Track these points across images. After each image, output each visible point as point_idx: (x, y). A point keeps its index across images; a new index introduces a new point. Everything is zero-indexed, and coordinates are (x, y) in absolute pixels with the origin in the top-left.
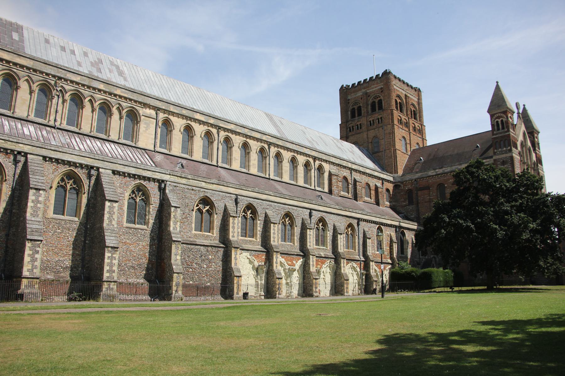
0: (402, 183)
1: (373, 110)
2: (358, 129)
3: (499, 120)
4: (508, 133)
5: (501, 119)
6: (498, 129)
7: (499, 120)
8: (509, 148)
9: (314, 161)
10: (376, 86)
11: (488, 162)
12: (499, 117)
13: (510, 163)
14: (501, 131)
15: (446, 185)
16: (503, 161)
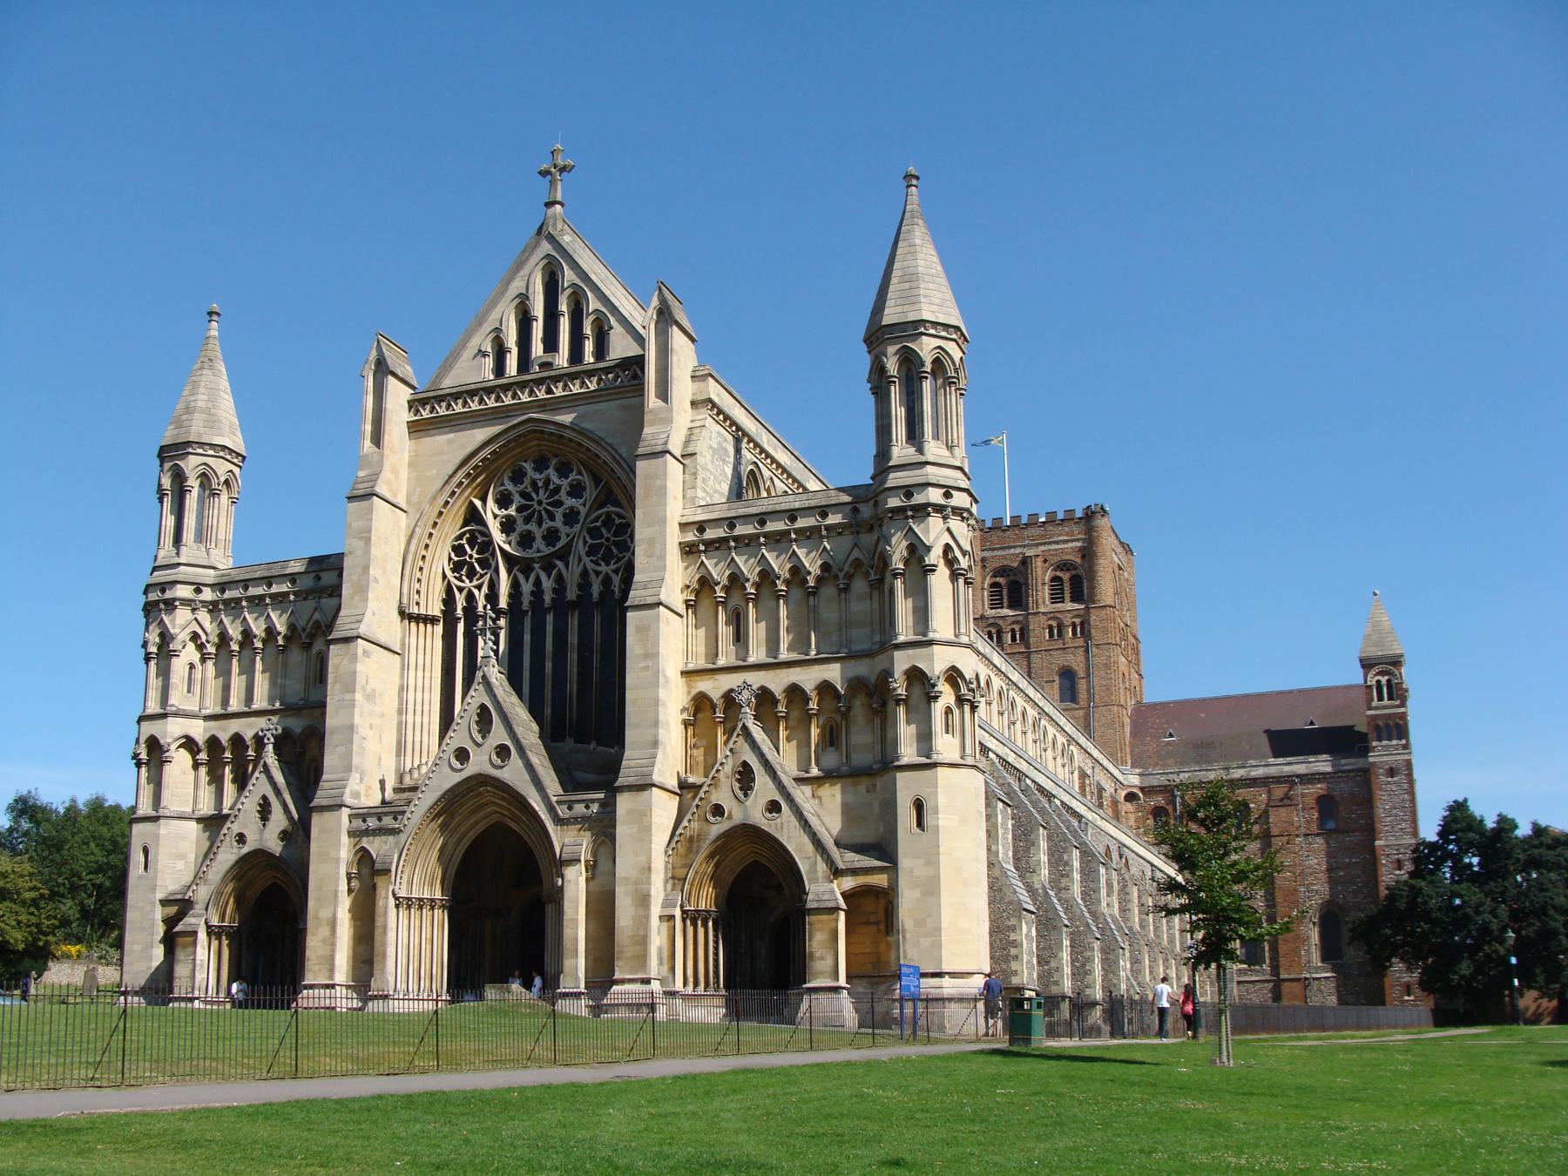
0: (1142, 789)
1: (1057, 597)
2: (1014, 639)
3: (1384, 680)
4: (1402, 710)
5: (1386, 678)
6: (1380, 698)
7: (1384, 680)
8: (1404, 742)
9: (1069, 745)
10: (1066, 538)
11: (1351, 764)
12: (1381, 673)
13: (1406, 775)
14: (1386, 702)
15: (1252, 805)
16: (1391, 769)
